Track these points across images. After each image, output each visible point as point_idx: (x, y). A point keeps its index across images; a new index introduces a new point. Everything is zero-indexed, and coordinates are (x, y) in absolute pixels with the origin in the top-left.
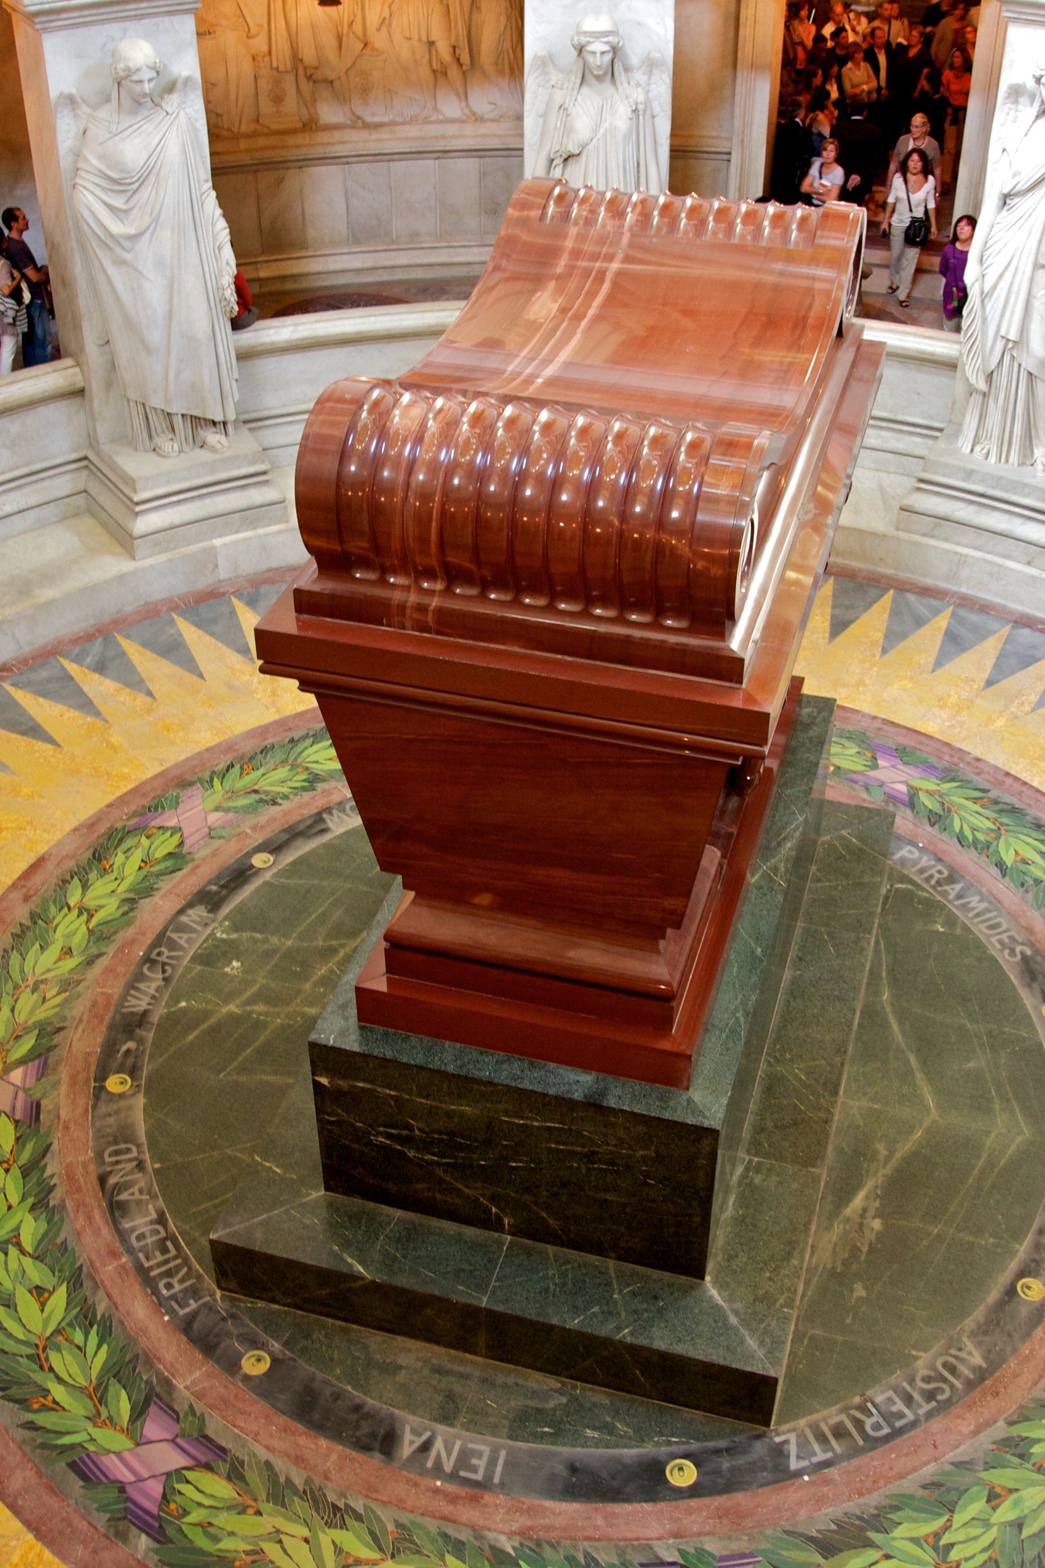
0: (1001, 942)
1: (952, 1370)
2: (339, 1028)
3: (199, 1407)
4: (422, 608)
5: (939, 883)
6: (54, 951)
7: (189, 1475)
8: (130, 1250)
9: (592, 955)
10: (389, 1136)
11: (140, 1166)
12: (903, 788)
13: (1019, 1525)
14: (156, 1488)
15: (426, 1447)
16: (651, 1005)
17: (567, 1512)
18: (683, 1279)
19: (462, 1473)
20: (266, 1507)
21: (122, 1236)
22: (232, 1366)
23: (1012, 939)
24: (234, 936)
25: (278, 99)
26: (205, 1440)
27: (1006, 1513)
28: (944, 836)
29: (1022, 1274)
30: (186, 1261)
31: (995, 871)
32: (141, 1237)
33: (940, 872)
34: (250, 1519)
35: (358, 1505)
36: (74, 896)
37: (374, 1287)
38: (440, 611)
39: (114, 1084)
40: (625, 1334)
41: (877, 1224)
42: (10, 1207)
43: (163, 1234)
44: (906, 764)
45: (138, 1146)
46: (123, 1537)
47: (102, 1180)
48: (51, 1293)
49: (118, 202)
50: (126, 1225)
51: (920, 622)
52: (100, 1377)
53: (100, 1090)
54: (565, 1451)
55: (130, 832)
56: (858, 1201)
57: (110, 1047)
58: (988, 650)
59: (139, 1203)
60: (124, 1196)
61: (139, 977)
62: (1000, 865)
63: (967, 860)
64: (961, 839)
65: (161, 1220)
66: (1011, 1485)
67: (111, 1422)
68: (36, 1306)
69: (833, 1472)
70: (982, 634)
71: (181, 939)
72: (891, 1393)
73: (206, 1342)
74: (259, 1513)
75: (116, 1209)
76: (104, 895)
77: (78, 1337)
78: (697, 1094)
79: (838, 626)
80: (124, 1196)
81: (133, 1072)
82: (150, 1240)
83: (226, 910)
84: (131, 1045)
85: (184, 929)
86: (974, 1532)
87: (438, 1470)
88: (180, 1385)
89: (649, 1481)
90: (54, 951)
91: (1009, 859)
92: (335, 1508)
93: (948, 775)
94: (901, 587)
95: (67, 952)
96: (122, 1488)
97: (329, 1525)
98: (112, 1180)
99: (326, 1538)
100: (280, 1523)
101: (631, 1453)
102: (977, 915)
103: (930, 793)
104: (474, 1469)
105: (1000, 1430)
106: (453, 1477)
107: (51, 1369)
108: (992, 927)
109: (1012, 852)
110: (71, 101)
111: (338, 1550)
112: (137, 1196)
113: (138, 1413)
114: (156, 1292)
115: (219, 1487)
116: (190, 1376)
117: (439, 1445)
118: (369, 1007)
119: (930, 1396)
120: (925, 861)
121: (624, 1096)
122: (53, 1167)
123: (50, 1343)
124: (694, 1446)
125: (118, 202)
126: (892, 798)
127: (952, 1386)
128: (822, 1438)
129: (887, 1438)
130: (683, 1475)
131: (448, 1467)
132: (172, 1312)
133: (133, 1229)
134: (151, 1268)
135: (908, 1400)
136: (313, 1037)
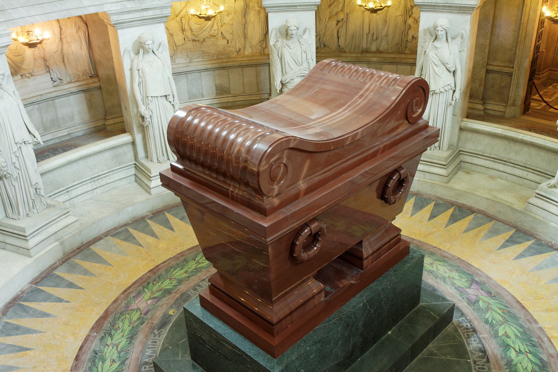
0: (159, 336)
11: (475, 362)
14: (472, 286)
23: (155, 336)
31: (127, 362)
33: (145, 368)
42: (520, 363)
43: (468, 340)
45: (475, 369)
47: (488, 361)
48: (503, 335)
59: (476, 351)
62: (123, 363)
67: (485, 302)
68: (508, 332)
77: (494, 322)
80: (481, 354)
82: (472, 339)
98: (485, 360)
100: (444, 274)
102: (154, 348)
108: (155, 342)
109: (112, 367)
111: (432, 267)
112: (476, 353)
113: (477, 301)
114: (471, 325)
133: (478, 343)
134: (473, 331)
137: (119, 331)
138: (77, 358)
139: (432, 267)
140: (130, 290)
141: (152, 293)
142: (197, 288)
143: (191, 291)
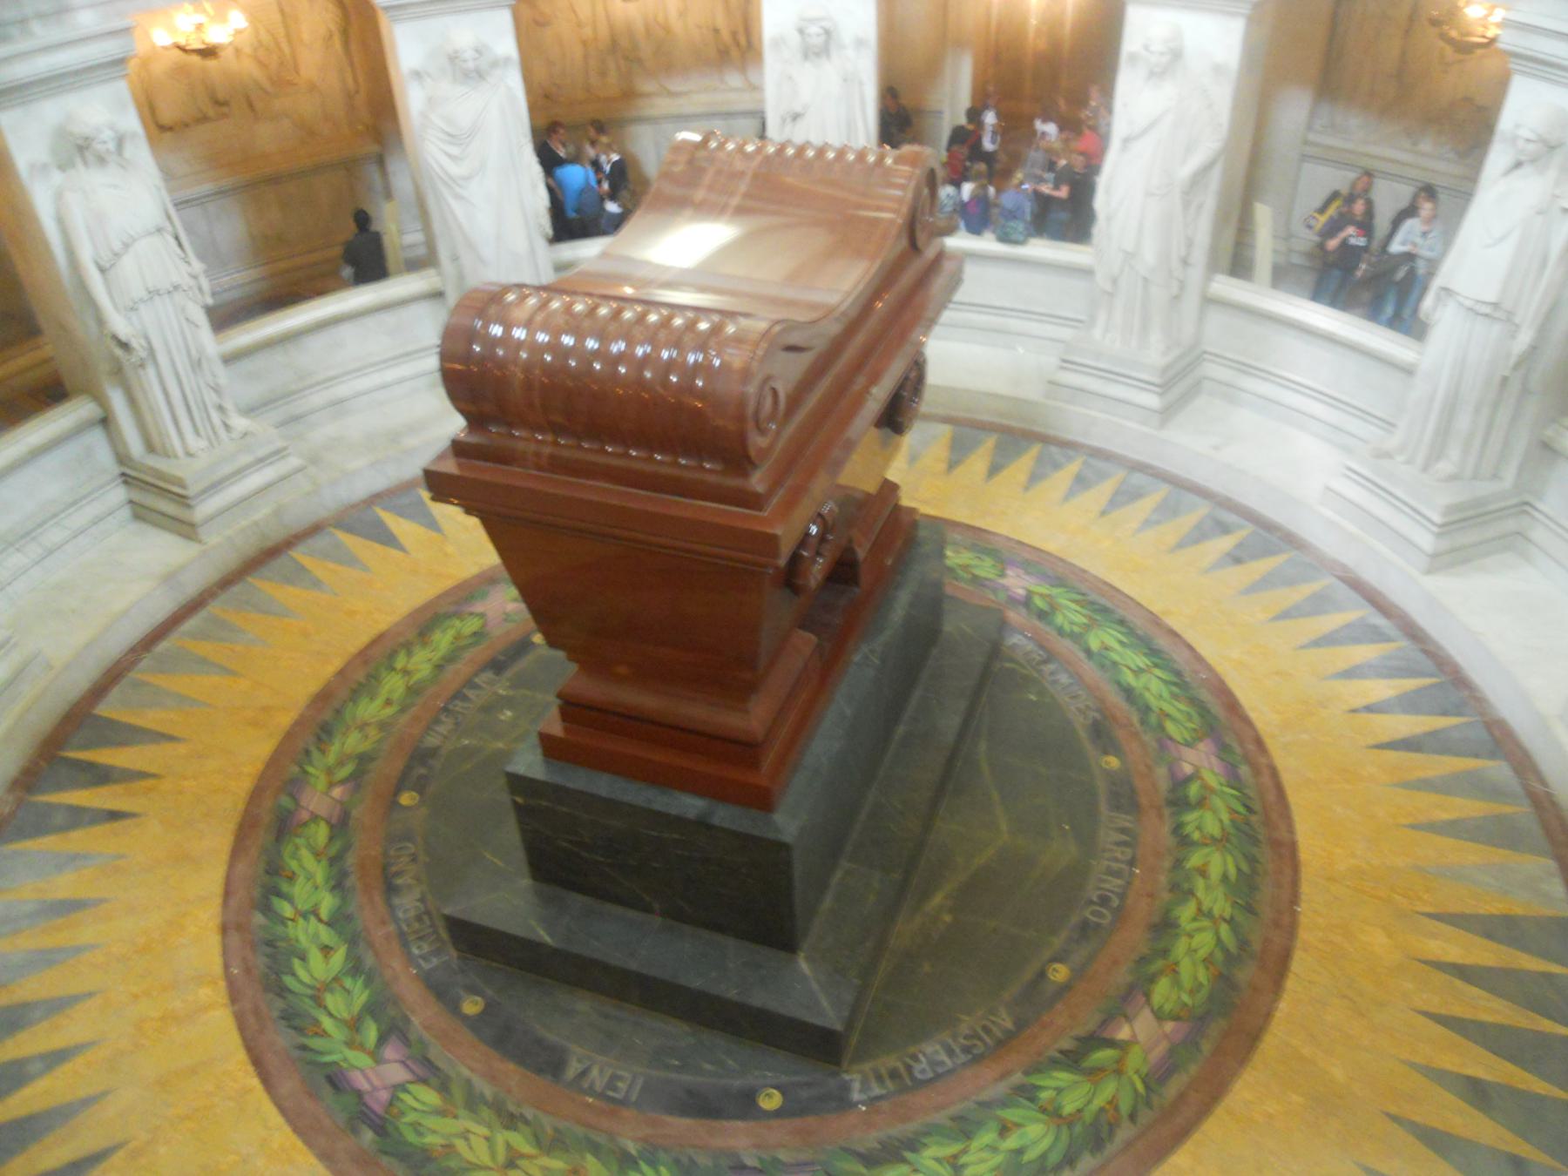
1: (986, 1030)
2: (529, 762)
3: (426, 1035)
4: (538, 455)
5: (1040, 663)
6: (379, 701)
7: (411, 1087)
8: (396, 921)
9: (698, 711)
10: (571, 842)
12: (1021, 592)
13: (1020, 1152)
14: (384, 1095)
15: (584, 1073)
16: (744, 750)
17: (681, 1125)
18: (783, 954)
19: (611, 1093)
20: (462, 1112)
21: (391, 908)
22: (454, 1008)
23: (1087, 707)
24: (511, 693)
25: (603, 74)
26: (427, 1063)
27: (1012, 1142)
28: (1048, 629)
29: (1055, 959)
30: (436, 932)
31: (1082, 655)
32: (406, 911)
34: (449, 1121)
35: (529, 1113)
36: (400, 662)
37: (555, 952)
38: (552, 457)
39: (407, 799)
40: (732, 994)
41: (948, 918)
44: (1028, 573)
46: (355, 1131)
49: (454, 151)
50: (396, 901)
51: (1057, 466)
52: (361, 1011)
53: (394, 804)
54: (687, 1078)
55: (448, 616)
56: (938, 899)
57: (408, 769)
58: (1106, 489)
59: (409, 887)
60: (399, 881)
61: (437, 721)
62: (1088, 652)
63: (1064, 646)
64: (1060, 631)
65: (422, 900)
66: (1016, 1119)
67: (361, 1047)
69: (885, 1105)
70: (1102, 476)
71: (471, 693)
72: (938, 1047)
73: (442, 991)
74: (455, 1117)
75: (391, 889)
76: (421, 662)
78: (779, 817)
79: (994, 470)
80: (399, 881)
81: (421, 792)
82: (412, 913)
83: (509, 673)
84: (423, 771)
85: (476, 687)
86: (985, 1155)
87: (591, 1091)
88: (415, 1020)
89: (745, 1105)
90: (379, 701)
91: (1094, 644)
92: (512, 1116)
93: (1059, 581)
94: (1045, 439)
95: (388, 702)
96: (359, 1094)
97: (507, 1128)
99: (503, 1137)
101: (737, 1083)
103: (1041, 595)
104: (615, 1089)
105: (1017, 1078)
106: (601, 1096)
107: (325, 1008)
110: (417, 75)
111: (508, 1146)
113: (382, 1039)
115: (430, 1097)
116: (423, 1013)
117: (595, 1072)
118: (551, 747)
119: (966, 1050)
120: (1030, 646)
121: (726, 816)
122: (351, 860)
123: (327, 987)
124: (784, 1079)
125: (454, 151)
126: (1013, 601)
127: (985, 1044)
128: (879, 1078)
129: (930, 1081)
130: (771, 1101)
131: (598, 1086)
132: (419, 966)
135: (951, 1053)
136: (511, 768)
137: (1166, 694)
138: (1174, 634)
139: (508, 1146)
140: (1266, 779)
141: (1205, 787)
142: (1124, 838)
143: (1128, 825)
